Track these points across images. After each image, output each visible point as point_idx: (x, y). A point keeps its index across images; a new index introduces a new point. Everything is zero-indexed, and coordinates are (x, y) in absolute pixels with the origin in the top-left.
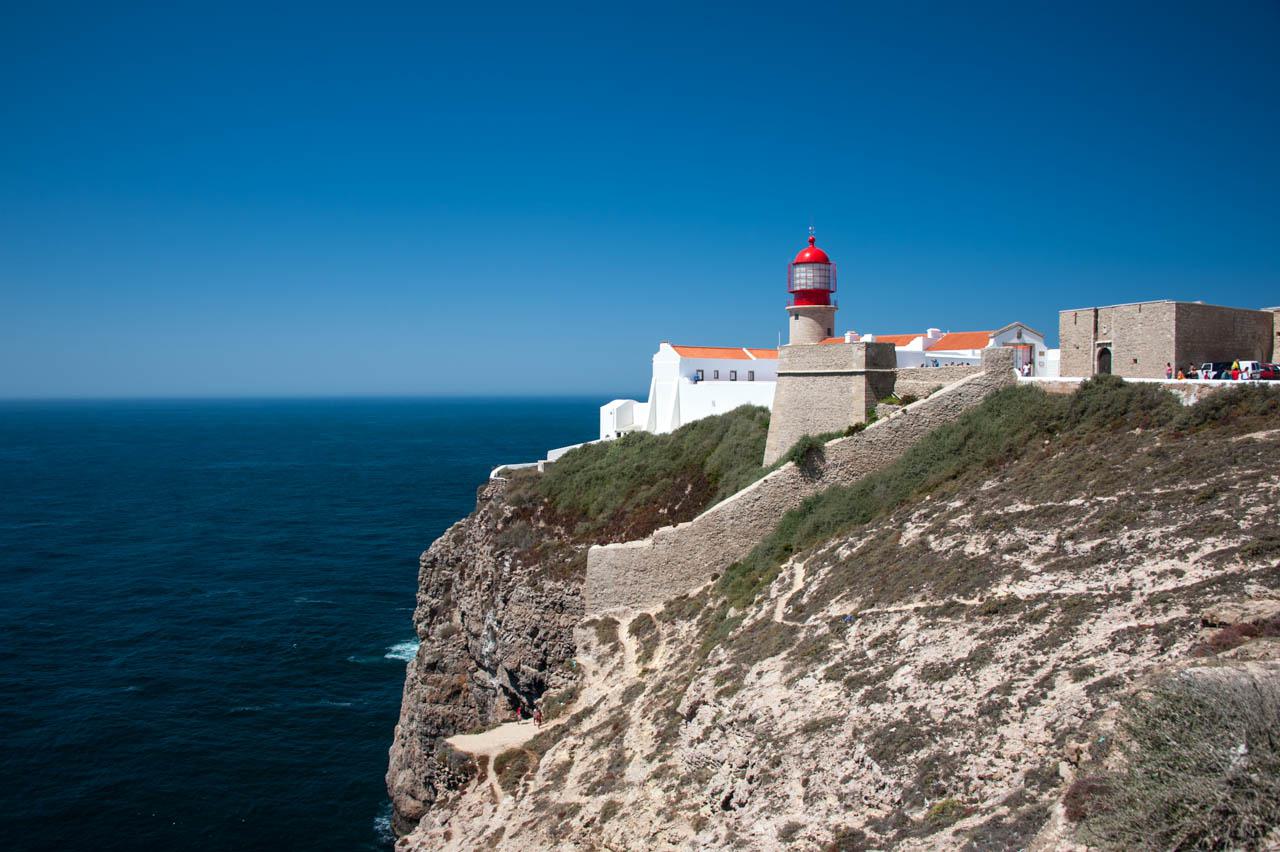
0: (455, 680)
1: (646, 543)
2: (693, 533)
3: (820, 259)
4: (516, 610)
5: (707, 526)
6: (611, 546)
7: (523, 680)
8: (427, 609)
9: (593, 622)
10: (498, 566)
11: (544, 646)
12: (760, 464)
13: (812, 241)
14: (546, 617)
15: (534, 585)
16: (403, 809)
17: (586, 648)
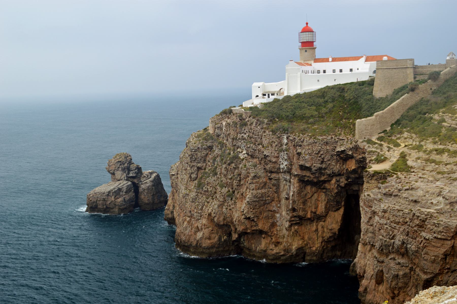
0: (264, 180)
6: (363, 119)
7: (314, 169)
8: (196, 168)
11: (323, 156)
13: (307, 24)
14: (323, 147)
16: (204, 245)
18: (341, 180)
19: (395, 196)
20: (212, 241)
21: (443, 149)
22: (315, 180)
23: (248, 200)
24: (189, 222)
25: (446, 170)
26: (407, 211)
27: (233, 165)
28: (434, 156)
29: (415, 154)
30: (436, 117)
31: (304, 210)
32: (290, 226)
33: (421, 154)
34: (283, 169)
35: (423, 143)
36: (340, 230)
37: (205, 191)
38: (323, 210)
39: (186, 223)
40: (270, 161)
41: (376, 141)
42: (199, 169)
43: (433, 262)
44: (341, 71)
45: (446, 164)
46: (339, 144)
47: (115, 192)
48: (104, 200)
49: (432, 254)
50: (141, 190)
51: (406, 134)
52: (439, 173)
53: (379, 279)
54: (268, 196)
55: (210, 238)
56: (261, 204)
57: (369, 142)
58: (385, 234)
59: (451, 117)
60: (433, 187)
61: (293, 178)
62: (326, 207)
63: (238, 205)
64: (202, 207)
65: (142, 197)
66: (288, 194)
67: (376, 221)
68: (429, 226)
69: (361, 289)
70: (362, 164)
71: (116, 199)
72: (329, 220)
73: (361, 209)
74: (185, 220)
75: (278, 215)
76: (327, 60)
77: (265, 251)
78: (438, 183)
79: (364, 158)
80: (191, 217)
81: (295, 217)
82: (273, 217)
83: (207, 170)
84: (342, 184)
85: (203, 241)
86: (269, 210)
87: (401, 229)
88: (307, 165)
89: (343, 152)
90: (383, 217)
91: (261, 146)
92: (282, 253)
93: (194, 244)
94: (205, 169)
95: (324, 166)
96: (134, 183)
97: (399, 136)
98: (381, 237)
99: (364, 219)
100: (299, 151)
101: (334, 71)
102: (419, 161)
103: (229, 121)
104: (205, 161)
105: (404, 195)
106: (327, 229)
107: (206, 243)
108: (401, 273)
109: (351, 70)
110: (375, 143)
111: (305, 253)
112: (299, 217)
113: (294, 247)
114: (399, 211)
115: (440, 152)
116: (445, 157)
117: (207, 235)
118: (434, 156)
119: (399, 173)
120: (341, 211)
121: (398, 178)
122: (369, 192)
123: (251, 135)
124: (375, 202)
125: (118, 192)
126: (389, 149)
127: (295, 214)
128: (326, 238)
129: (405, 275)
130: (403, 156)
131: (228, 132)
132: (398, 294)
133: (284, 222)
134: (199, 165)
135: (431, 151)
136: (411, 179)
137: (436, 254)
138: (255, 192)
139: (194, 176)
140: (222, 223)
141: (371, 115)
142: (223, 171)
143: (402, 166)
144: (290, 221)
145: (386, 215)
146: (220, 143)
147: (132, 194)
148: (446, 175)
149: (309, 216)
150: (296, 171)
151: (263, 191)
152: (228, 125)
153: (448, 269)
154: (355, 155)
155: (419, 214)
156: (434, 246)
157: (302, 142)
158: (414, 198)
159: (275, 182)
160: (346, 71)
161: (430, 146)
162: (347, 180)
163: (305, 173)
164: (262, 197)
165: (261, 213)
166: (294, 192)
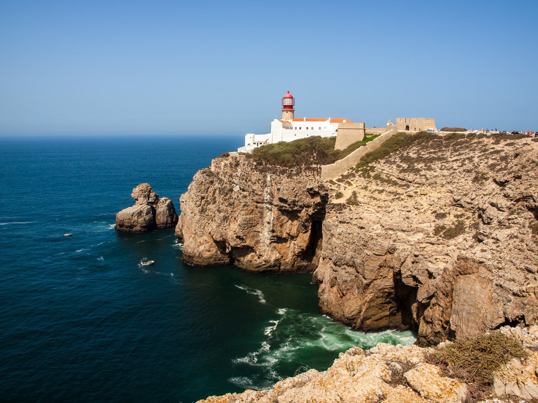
0: (252, 208)
1: (334, 164)
2: (344, 161)
3: (291, 97)
4: (285, 185)
5: (346, 160)
7: (289, 201)
9: (327, 182)
10: (265, 176)
12: (334, 148)
15: (291, 178)
16: (204, 256)
17: (331, 186)
18: (309, 210)
19: (348, 223)
20: (210, 253)
21: (383, 190)
22: (290, 210)
23: (239, 223)
24: (193, 238)
25: (384, 205)
26: (355, 234)
27: (228, 195)
28: (376, 195)
29: (363, 192)
30: (379, 166)
31: (281, 232)
32: (270, 243)
33: (368, 193)
34: (267, 200)
35: (368, 185)
36: (307, 247)
37: (207, 215)
38: (295, 232)
39: (191, 238)
40: (257, 194)
41: (336, 182)
42: (203, 198)
43: (372, 271)
44: (312, 128)
45: (384, 201)
46: (309, 183)
47: (138, 213)
48: (129, 219)
49: (371, 265)
50: (157, 212)
51: (357, 178)
52: (379, 207)
53: (333, 283)
54: (255, 221)
55: (209, 251)
56: (250, 225)
57: (331, 182)
58: (339, 251)
59: (389, 167)
60: (373, 217)
61: (274, 207)
62: (297, 230)
63: (232, 226)
64: (204, 227)
65: (159, 217)
66: (270, 220)
67: (333, 241)
68: (370, 245)
69: (320, 290)
70: (325, 199)
71: (138, 219)
72: (299, 239)
73: (323, 232)
74: (191, 236)
75: (261, 234)
76: (302, 120)
77: (251, 261)
78: (378, 214)
79: (327, 195)
80: (196, 234)
81: (274, 236)
82: (257, 236)
83: (208, 199)
84: (310, 213)
85: (204, 252)
86: (255, 231)
87: (351, 248)
88: (285, 198)
89: (311, 189)
90: (338, 238)
91: (250, 182)
92: (264, 263)
93: (197, 254)
94: (207, 198)
95: (297, 199)
96: (152, 208)
97: (352, 179)
98: (336, 253)
99: (324, 239)
100: (279, 187)
101: (307, 128)
102: (366, 198)
103: (227, 162)
104: (207, 192)
105: (354, 222)
106: (298, 246)
107: (207, 254)
108: (349, 279)
109: (320, 128)
110: (336, 183)
111: (280, 264)
112: (277, 236)
113: (273, 259)
114: (349, 234)
115: (381, 192)
116: (383, 196)
117: (207, 248)
118: (376, 195)
119: (351, 206)
120: (309, 233)
121: (350, 210)
122: (330, 220)
123: (243, 173)
124: (334, 227)
125: (140, 213)
126: (345, 188)
127: (274, 234)
128: (297, 252)
129: (352, 280)
130: (354, 194)
131: (226, 171)
132: (346, 294)
133: (266, 240)
134: (203, 195)
135: (375, 191)
136: (359, 211)
137: (374, 265)
138: (244, 217)
139: (198, 203)
140: (219, 240)
141: (333, 162)
142: (221, 200)
143: (353, 201)
144: (270, 240)
145: (341, 237)
146: (219, 179)
147: (151, 215)
148: (384, 209)
149: (285, 235)
150: (276, 202)
151: (251, 216)
152: (226, 165)
153: (381, 276)
154: (320, 192)
155: (363, 237)
156: (373, 260)
157: (282, 180)
158: (361, 225)
159: (261, 210)
160: (316, 129)
161: (373, 187)
162: (314, 210)
163: (282, 204)
164: (250, 220)
165: (248, 233)
166: (274, 218)
